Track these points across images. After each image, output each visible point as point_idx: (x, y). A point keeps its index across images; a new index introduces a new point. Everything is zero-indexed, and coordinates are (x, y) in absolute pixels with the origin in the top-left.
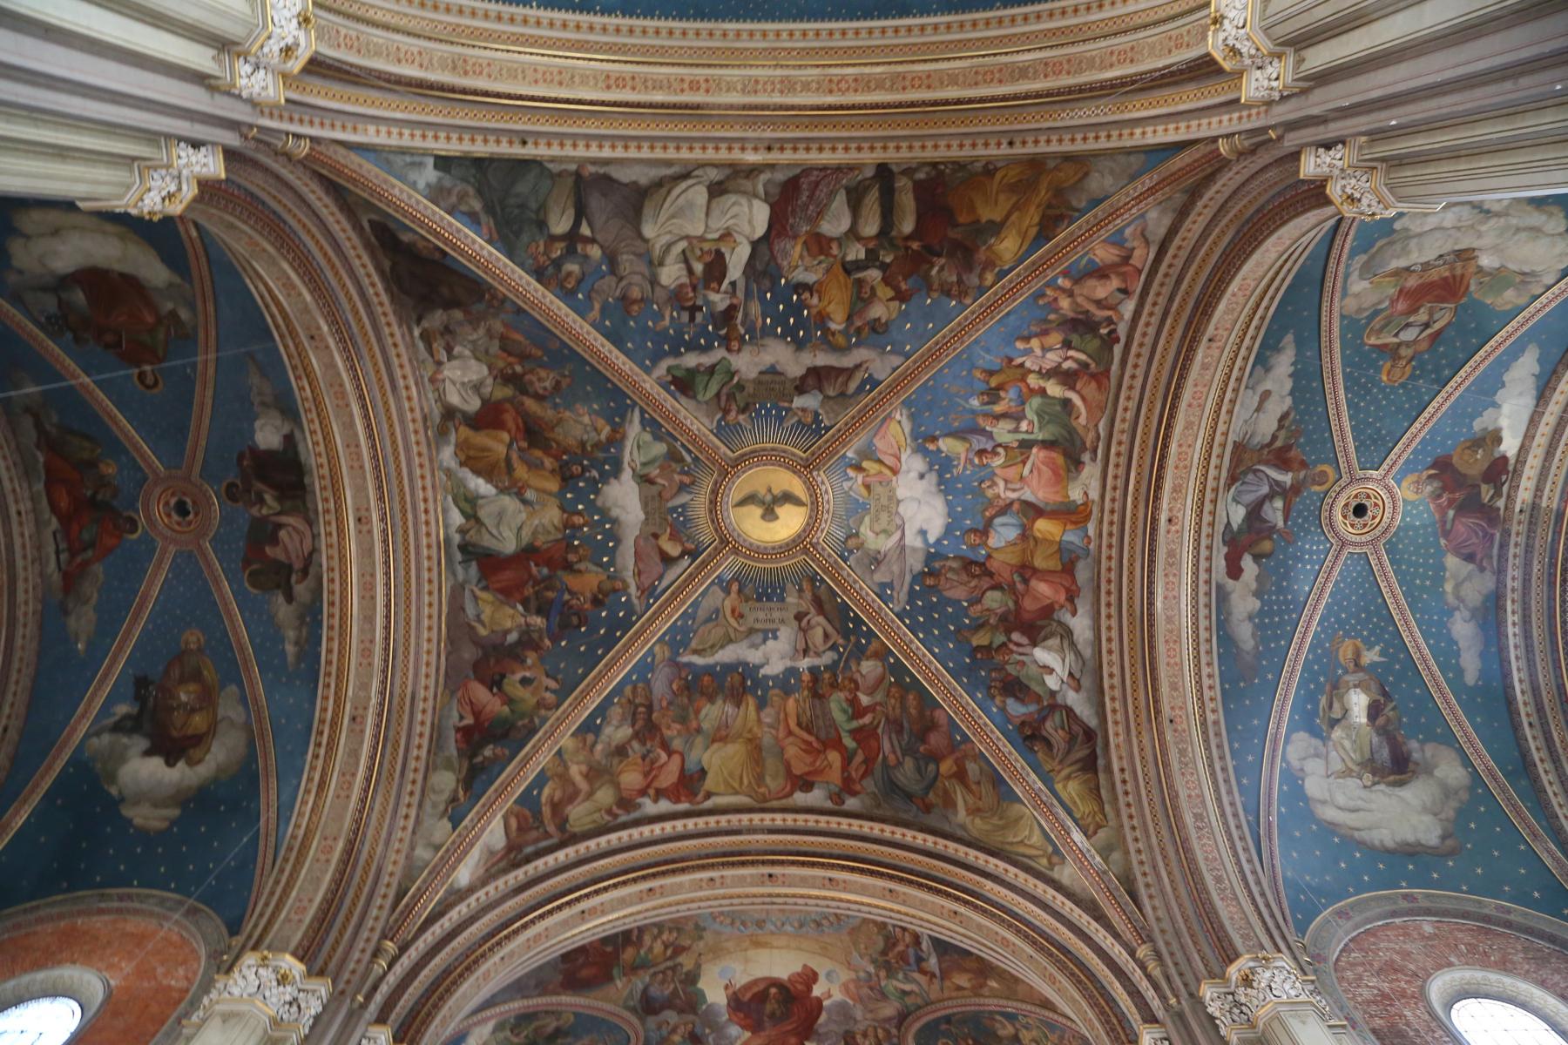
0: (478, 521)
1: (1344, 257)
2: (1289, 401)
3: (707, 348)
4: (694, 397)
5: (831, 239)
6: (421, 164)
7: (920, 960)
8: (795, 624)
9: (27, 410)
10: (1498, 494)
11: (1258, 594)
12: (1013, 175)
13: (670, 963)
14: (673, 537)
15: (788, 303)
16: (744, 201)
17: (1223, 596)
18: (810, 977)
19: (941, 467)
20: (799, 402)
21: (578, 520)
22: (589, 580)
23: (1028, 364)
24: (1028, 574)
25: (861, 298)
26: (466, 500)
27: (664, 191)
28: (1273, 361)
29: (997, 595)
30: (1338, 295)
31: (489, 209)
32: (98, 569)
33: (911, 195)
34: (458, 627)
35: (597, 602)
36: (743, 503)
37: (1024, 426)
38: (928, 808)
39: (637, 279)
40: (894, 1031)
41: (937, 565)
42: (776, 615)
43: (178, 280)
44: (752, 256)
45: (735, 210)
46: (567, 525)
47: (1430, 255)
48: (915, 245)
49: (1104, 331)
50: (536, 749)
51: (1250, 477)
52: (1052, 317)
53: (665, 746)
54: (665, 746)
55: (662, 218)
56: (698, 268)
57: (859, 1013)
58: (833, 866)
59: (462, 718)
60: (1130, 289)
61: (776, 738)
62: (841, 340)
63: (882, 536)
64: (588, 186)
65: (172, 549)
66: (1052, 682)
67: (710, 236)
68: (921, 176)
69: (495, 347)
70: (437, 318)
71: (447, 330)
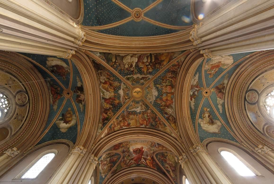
0: (104, 95)
1: (205, 63)
2: (198, 80)
3: (130, 75)
4: (129, 81)
5: (145, 62)
6: (98, 53)
7: (155, 146)
8: (141, 106)
9: (48, 82)
10: (224, 90)
11: (194, 102)
12: (166, 54)
13: (126, 146)
14: (127, 96)
15: (140, 70)
16: (134, 58)
17: (190, 103)
18: (142, 148)
19: (157, 88)
20: (141, 81)
21: (116, 95)
22: (117, 101)
23: (167, 76)
24: (167, 100)
25: (148, 69)
26: (103, 92)
27: (125, 57)
28: (196, 75)
29: (164, 103)
30: (204, 68)
31: (106, 59)
32: (57, 101)
33: (154, 57)
34: (102, 107)
35: (118, 104)
36: (134, 92)
37: (167, 83)
38: (156, 127)
39: (123, 67)
40: (152, 154)
41: (157, 99)
42: (139, 105)
43: (68, 66)
44: (136, 64)
45: (134, 59)
46: (114, 95)
47: (215, 62)
48: (154, 63)
49: (176, 72)
50: (111, 121)
51: (193, 89)
52: (170, 71)
53: (126, 120)
54: (126, 120)
55: (126, 59)
56: (130, 66)
57: (148, 152)
58: (145, 134)
59: (102, 118)
60: (179, 67)
61: (138, 119)
62: (146, 74)
63: (150, 96)
64: (117, 56)
65: (67, 98)
66: (170, 113)
67: (131, 62)
68: (155, 55)
69: (106, 75)
70: (100, 71)
71: (101, 73)
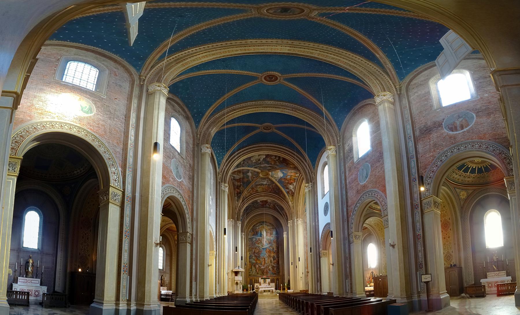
19: (283, 173)
